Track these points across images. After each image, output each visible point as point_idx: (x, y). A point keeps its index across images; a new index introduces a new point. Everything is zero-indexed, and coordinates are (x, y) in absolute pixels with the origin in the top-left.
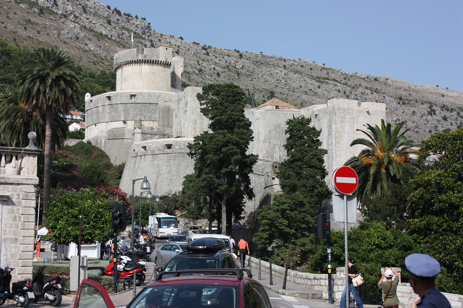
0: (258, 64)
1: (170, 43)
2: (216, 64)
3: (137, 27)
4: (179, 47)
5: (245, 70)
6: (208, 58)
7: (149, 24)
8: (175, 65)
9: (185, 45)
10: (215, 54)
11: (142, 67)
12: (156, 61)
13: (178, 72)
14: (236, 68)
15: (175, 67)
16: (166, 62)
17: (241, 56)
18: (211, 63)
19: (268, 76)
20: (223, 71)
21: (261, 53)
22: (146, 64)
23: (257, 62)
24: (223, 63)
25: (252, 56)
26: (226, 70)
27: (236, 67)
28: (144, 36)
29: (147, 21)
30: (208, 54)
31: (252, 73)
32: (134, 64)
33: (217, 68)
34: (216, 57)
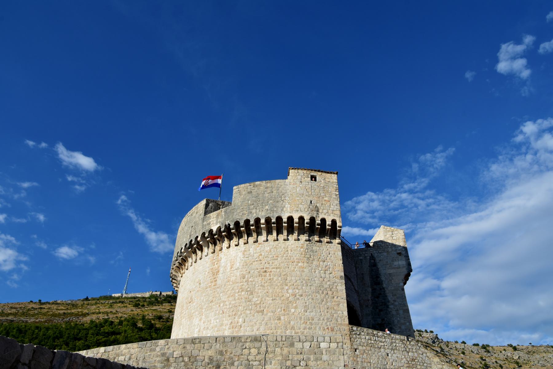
0: (531, 353)
1: (455, 347)
2: (496, 358)
3: (427, 338)
4: (463, 349)
5: (522, 360)
6: (489, 354)
7: (437, 335)
8: (376, 255)
9: (468, 348)
10: (493, 351)
11: (222, 255)
12: (268, 220)
13: (390, 274)
14: (513, 359)
15: (377, 260)
16: (313, 220)
17: (515, 349)
18: (492, 358)
19: (544, 361)
20: (504, 363)
21: (530, 344)
22: (234, 241)
23: (530, 352)
24: (502, 357)
25: (524, 348)
26: (506, 362)
27: (514, 358)
28: (434, 345)
29: (435, 333)
30: (489, 352)
31: (528, 361)
32: (199, 253)
33: (498, 362)
34: (495, 353)
